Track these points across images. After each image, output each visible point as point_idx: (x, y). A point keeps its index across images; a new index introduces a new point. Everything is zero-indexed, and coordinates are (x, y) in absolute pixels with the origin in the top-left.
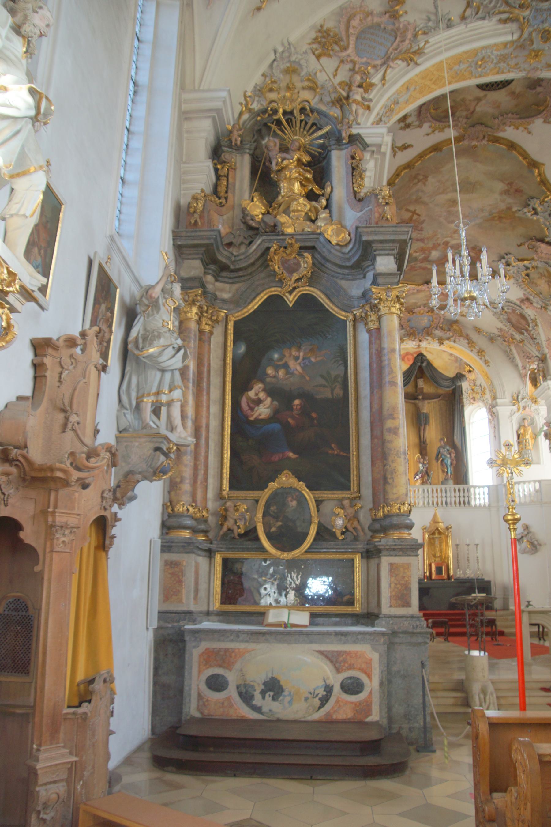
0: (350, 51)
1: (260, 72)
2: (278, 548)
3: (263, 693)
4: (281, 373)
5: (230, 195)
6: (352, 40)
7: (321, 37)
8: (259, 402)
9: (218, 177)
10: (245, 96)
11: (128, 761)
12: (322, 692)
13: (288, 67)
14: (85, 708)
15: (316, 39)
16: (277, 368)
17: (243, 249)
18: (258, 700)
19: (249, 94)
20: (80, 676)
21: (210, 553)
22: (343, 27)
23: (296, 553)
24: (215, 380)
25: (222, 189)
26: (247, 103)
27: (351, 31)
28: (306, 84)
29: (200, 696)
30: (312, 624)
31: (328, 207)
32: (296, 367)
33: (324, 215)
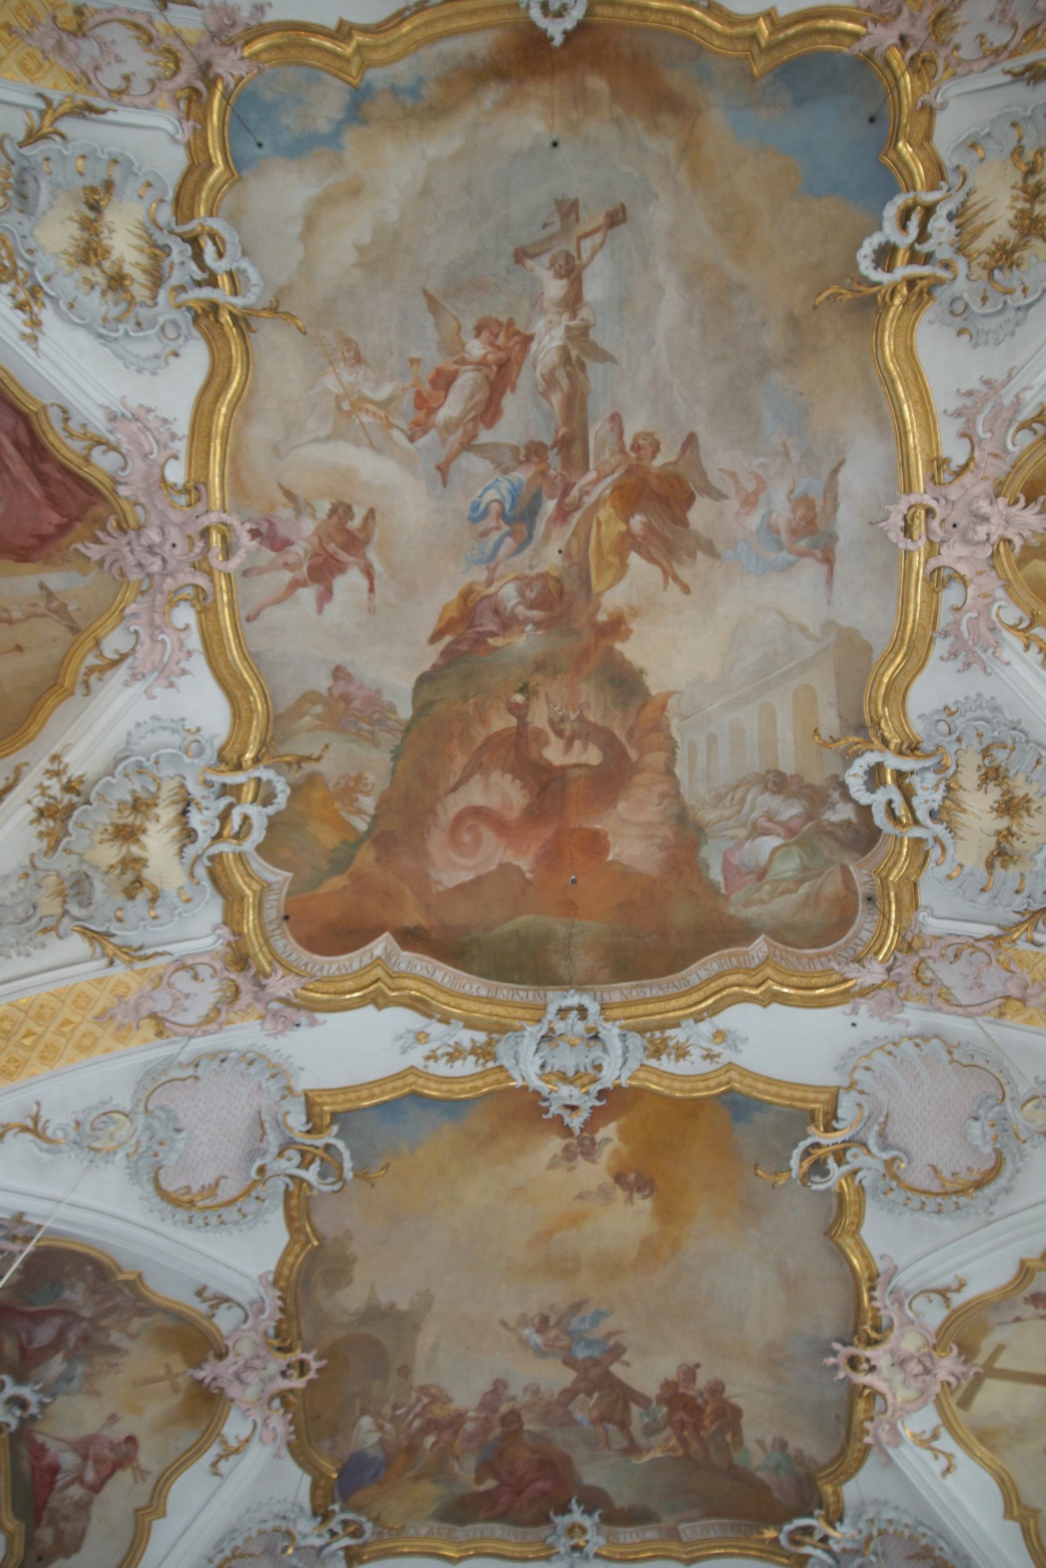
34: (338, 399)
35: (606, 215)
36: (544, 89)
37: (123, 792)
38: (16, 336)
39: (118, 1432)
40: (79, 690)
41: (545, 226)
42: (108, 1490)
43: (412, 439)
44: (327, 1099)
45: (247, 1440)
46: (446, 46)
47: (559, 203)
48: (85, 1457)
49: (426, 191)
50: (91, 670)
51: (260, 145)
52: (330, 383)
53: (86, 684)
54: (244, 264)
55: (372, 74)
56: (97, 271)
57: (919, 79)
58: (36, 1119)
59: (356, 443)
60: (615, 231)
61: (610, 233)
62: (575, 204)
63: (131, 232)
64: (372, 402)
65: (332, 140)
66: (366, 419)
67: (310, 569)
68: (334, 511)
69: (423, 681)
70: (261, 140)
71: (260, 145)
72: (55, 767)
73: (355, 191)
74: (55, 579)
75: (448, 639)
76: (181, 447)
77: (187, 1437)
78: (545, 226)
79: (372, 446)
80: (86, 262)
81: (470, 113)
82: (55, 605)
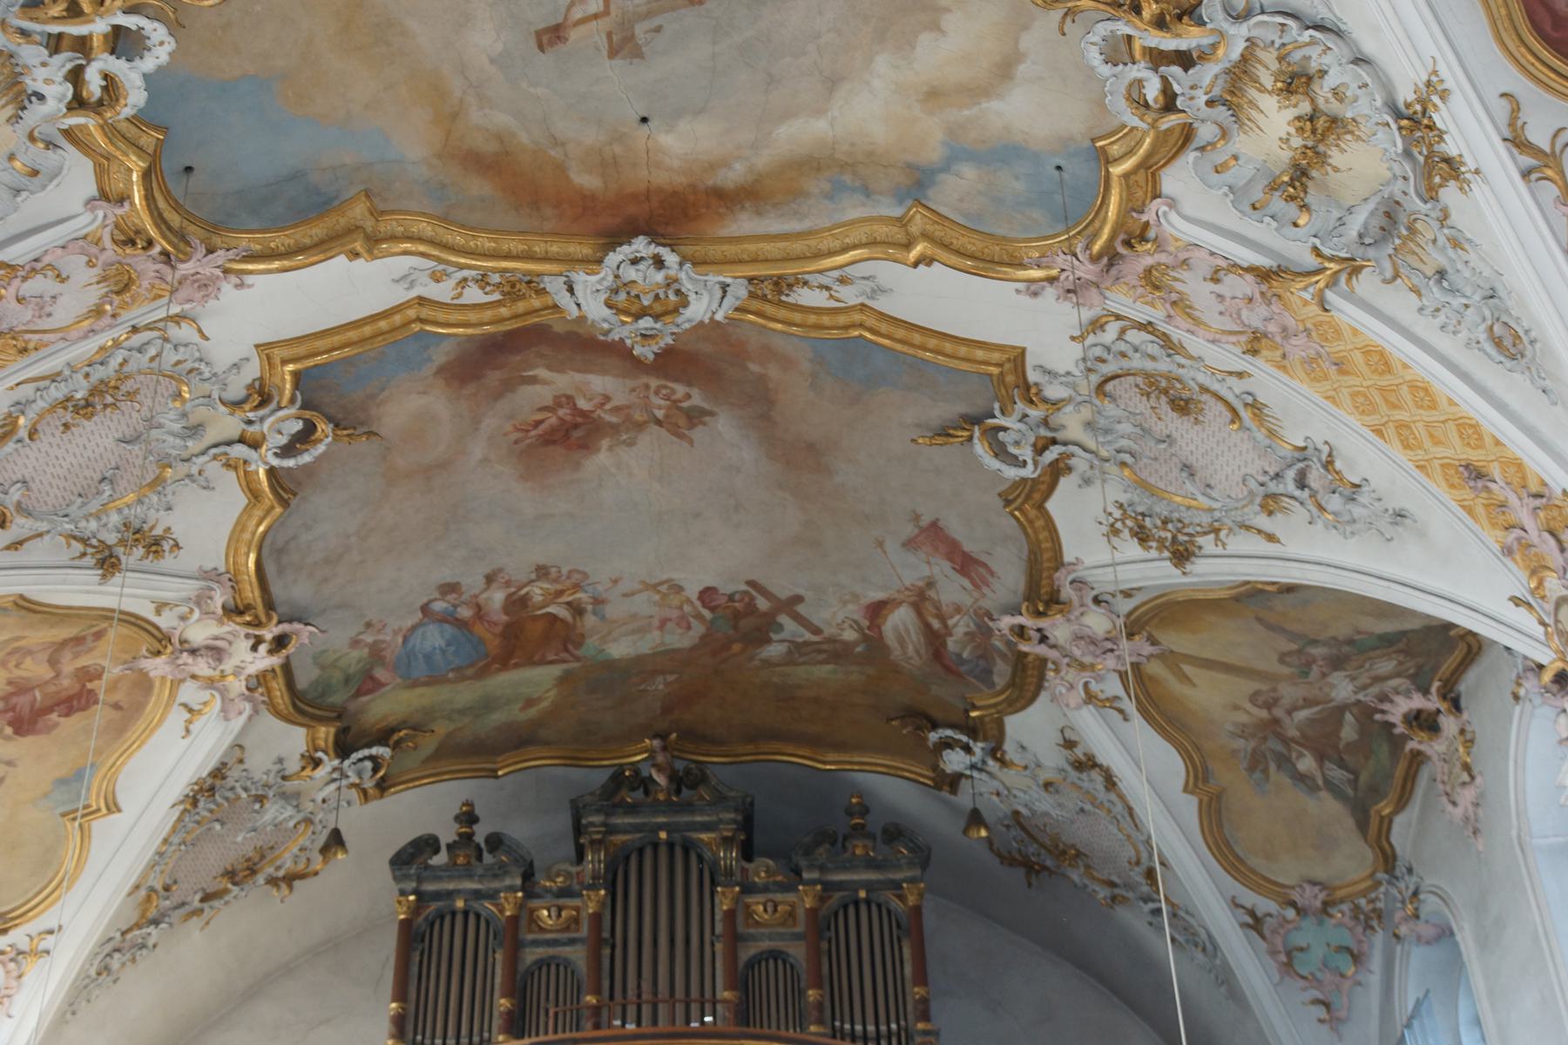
35: (567, 39)
36: (661, 178)
38: (1456, 100)
41: (658, 29)
46: (794, 226)
47: (637, 54)
49: (832, 83)
51: (1059, 168)
55: (897, 212)
56: (1321, 102)
57: (134, 225)
60: (552, 22)
61: (560, 20)
62: (613, 53)
65: (956, 155)
70: (1056, 173)
71: (1059, 168)
73: (934, 95)
78: (658, 29)
80: (1334, 120)
81: (764, 160)
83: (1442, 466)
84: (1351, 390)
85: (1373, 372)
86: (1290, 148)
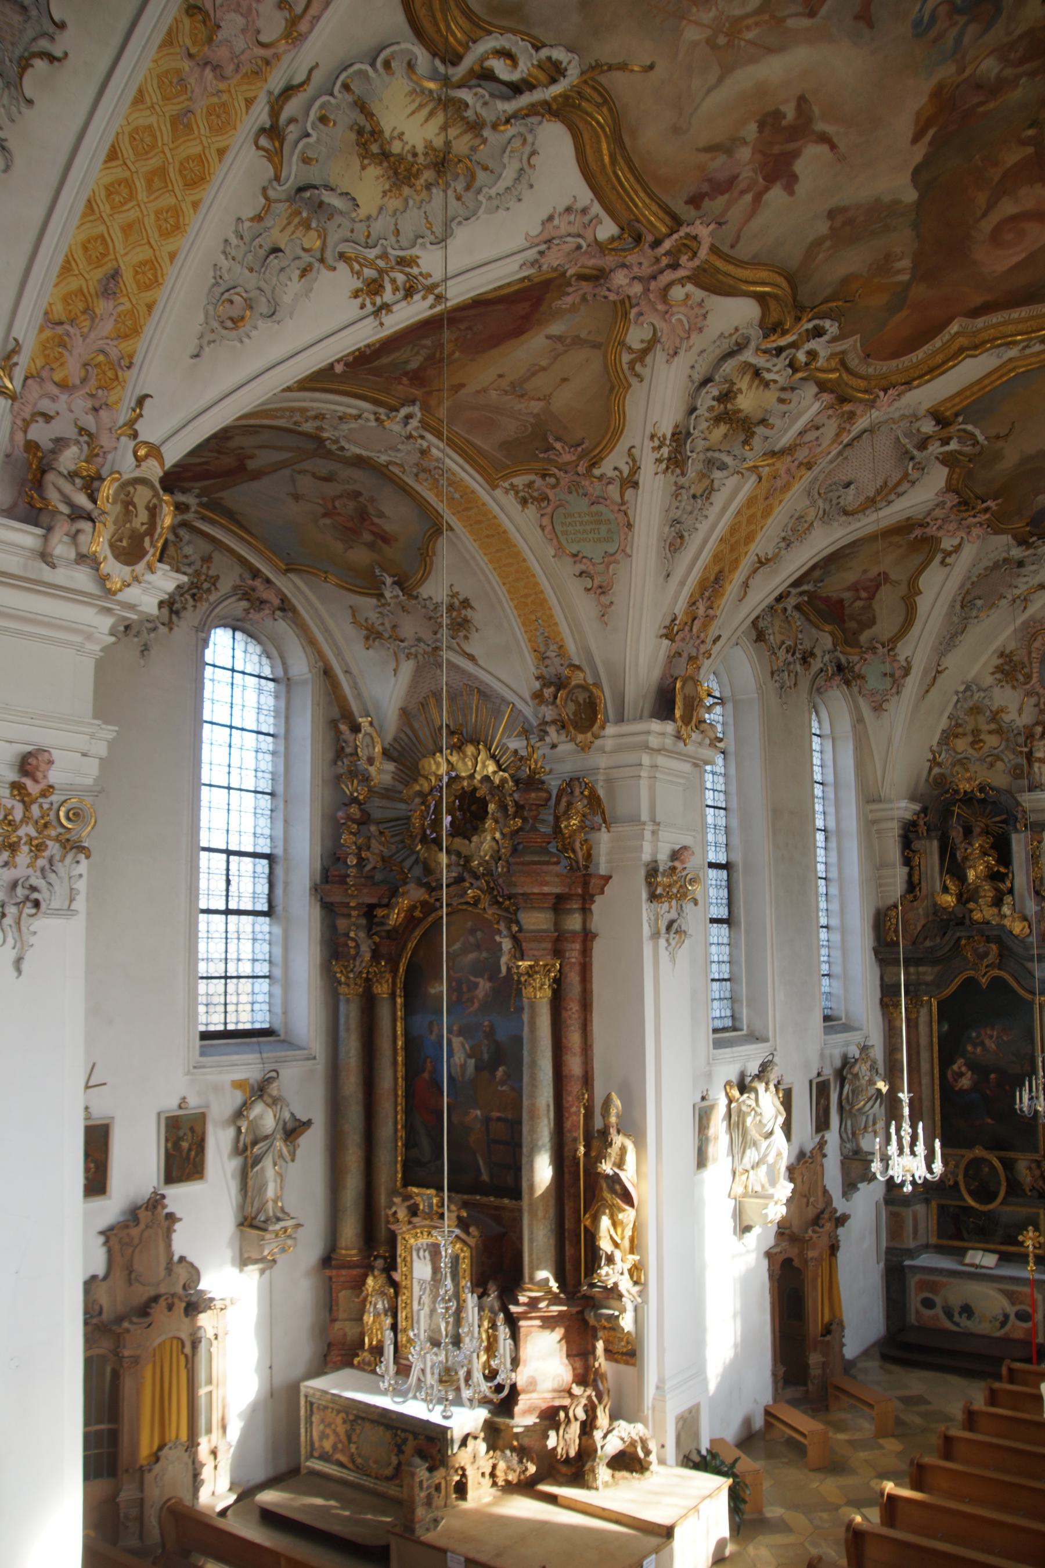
0: (1034, 680)
1: (946, 714)
2: (977, 1202)
3: (960, 1314)
4: (979, 1050)
5: (923, 884)
6: (1036, 666)
7: (1006, 663)
8: (961, 1075)
9: (911, 869)
10: (933, 752)
11: (866, 1353)
12: (1001, 1318)
13: (971, 709)
14: (828, 1338)
15: (997, 667)
16: (975, 1045)
17: (938, 940)
18: (957, 1318)
19: (935, 748)
20: (826, 1319)
21: (927, 1201)
22: (1024, 652)
23: (991, 1207)
24: (924, 1055)
25: (916, 878)
26: (934, 758)
27: (1034, 655)
28: (993, 726)
29: (917, 1312)
30: (997, 1266)
31: (1011, 891)
32: (991, 1045)
33: (1008, 899)
34: (711, 43)
37: (706, 400)
39: (873, 572)
40: (634, 381)
42: (878, 596)
43: (812, 14)
44: (948, 405)
45: (960, 545)
48: (857, 590)
50: (632, 364)
52: (692, 34)
53: (638, 376)
54: (544, 53)
58: (760, 562)
59: (753, 60)
63: (413, 113)
64: (747, 16)
66: (750, 35)
67: (764, 179)
68: (762, 125)
69: (917, 172)
72: (657, 443)
74: (556, 328)
75: (931, 132)
76: (597, 209)
77: (917, 559)
79: (770, 50)
82: (568, 341)
83: (102, 236)
84: (155, 125)
85: (181, 164)
86: (392, 138)
